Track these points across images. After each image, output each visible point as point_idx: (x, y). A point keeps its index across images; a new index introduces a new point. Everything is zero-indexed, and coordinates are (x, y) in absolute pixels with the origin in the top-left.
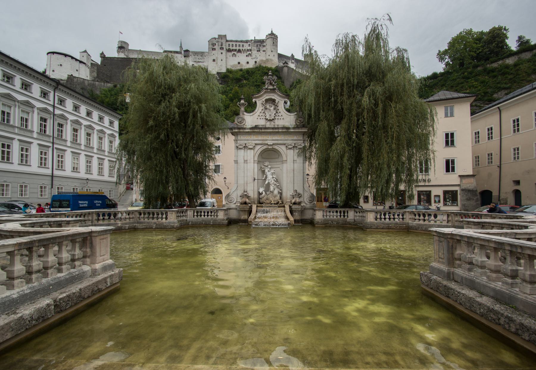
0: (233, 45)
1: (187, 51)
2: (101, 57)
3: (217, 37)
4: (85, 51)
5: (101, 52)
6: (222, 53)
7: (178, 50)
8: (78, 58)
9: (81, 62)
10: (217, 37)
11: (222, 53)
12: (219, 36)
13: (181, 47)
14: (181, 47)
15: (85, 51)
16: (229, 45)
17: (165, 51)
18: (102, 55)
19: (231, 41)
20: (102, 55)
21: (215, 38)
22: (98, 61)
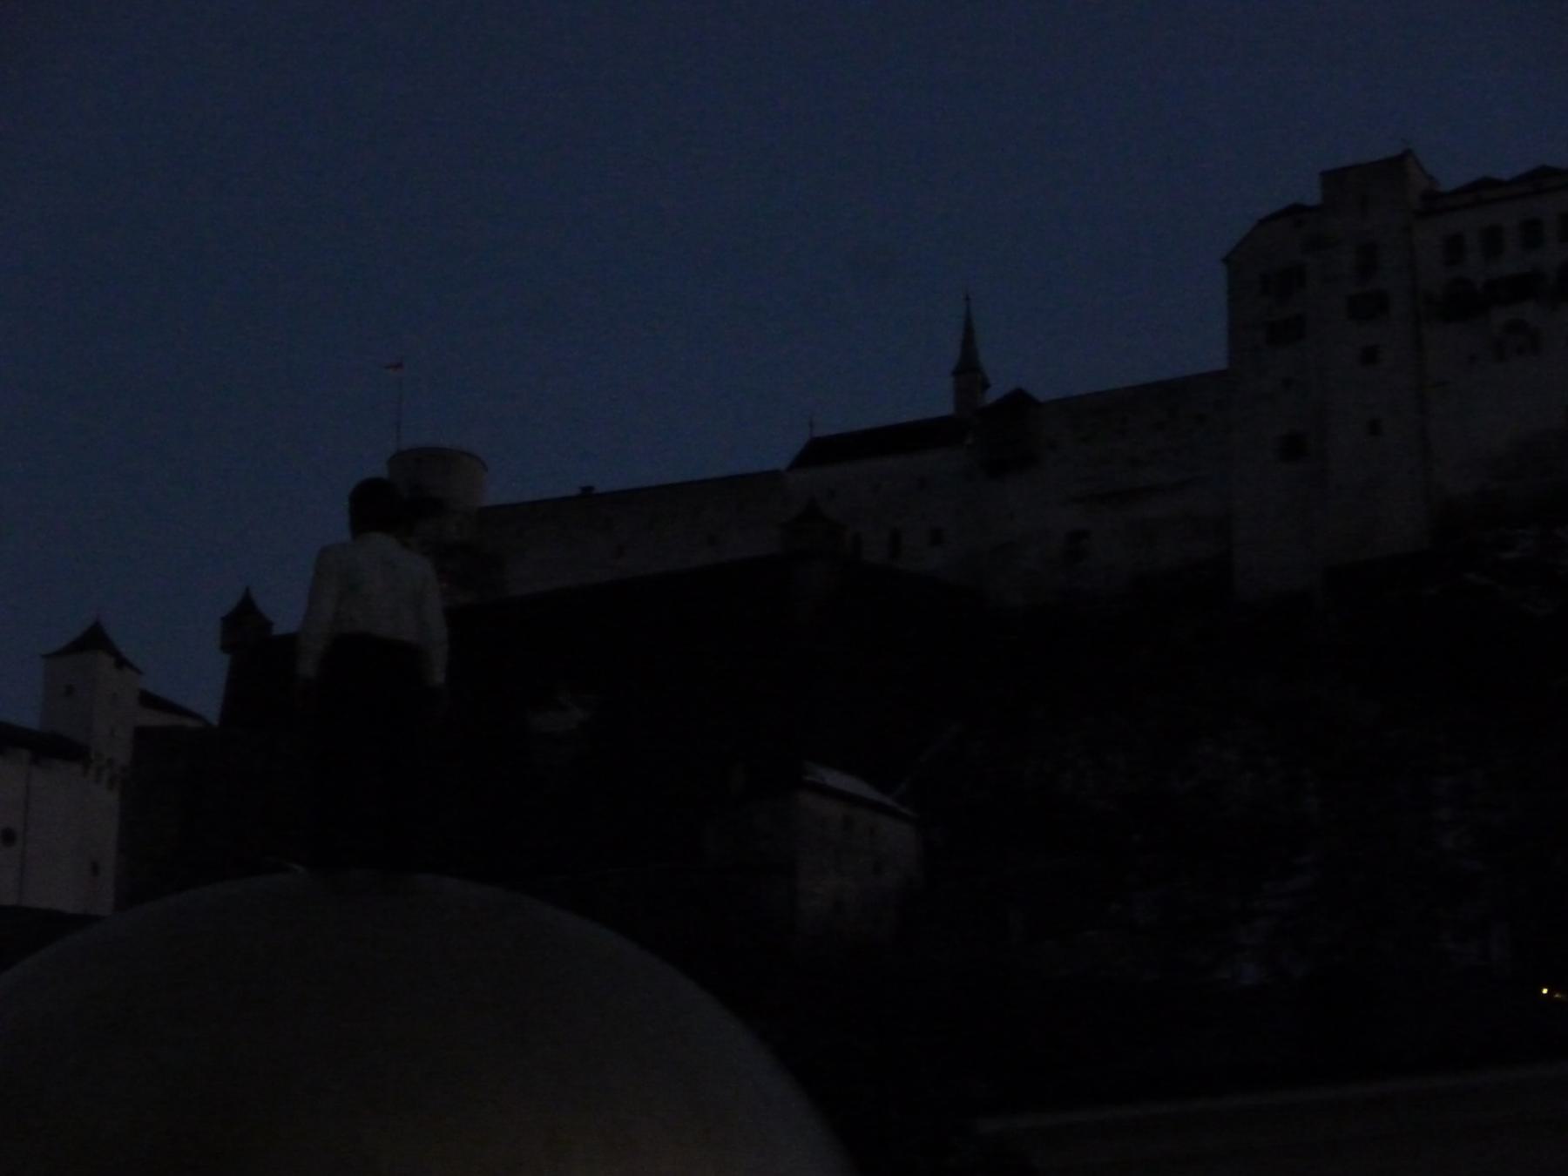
0: (1492, 240)
1: (1019, 401)
2: (225, 648)
3: (1312, 195)
4: (94, 639)
5: (231, 603)
6: (1370, 356)
7: (939, 402)
8: (28, 717)
9: (50, 747)
10: (1312, 195)
11: (1370, 356)
12: (1333, 179)
13: (968, 370)
14: (968, 370)
15: (94, 639)
16: (1454, 247)
17: (820, 452)
18: (244, 627)
19: (1481, 191)
20: (244, 627)
21: (1295, 212)
22: (200, 685)
